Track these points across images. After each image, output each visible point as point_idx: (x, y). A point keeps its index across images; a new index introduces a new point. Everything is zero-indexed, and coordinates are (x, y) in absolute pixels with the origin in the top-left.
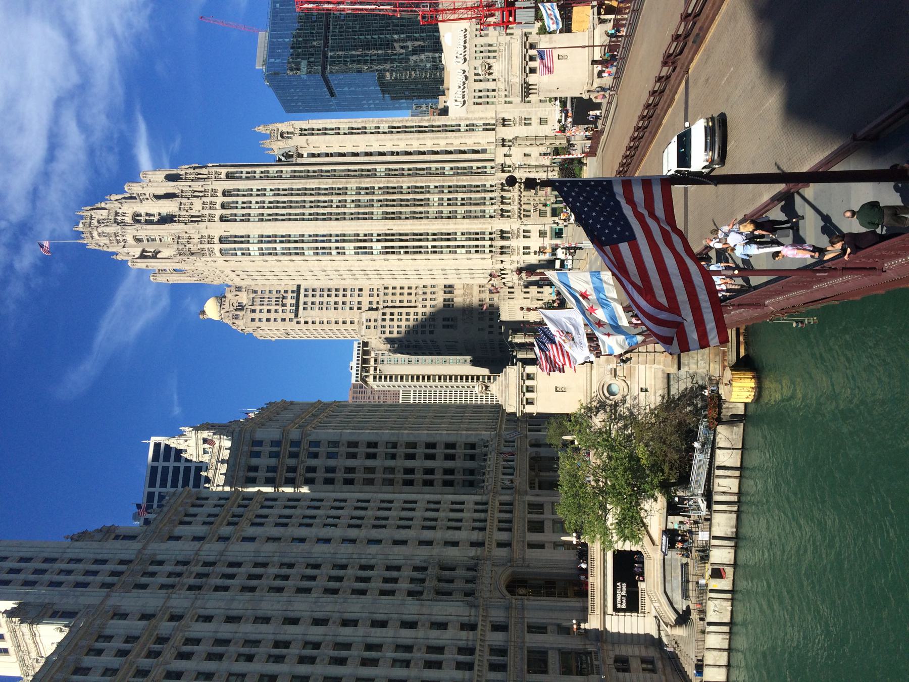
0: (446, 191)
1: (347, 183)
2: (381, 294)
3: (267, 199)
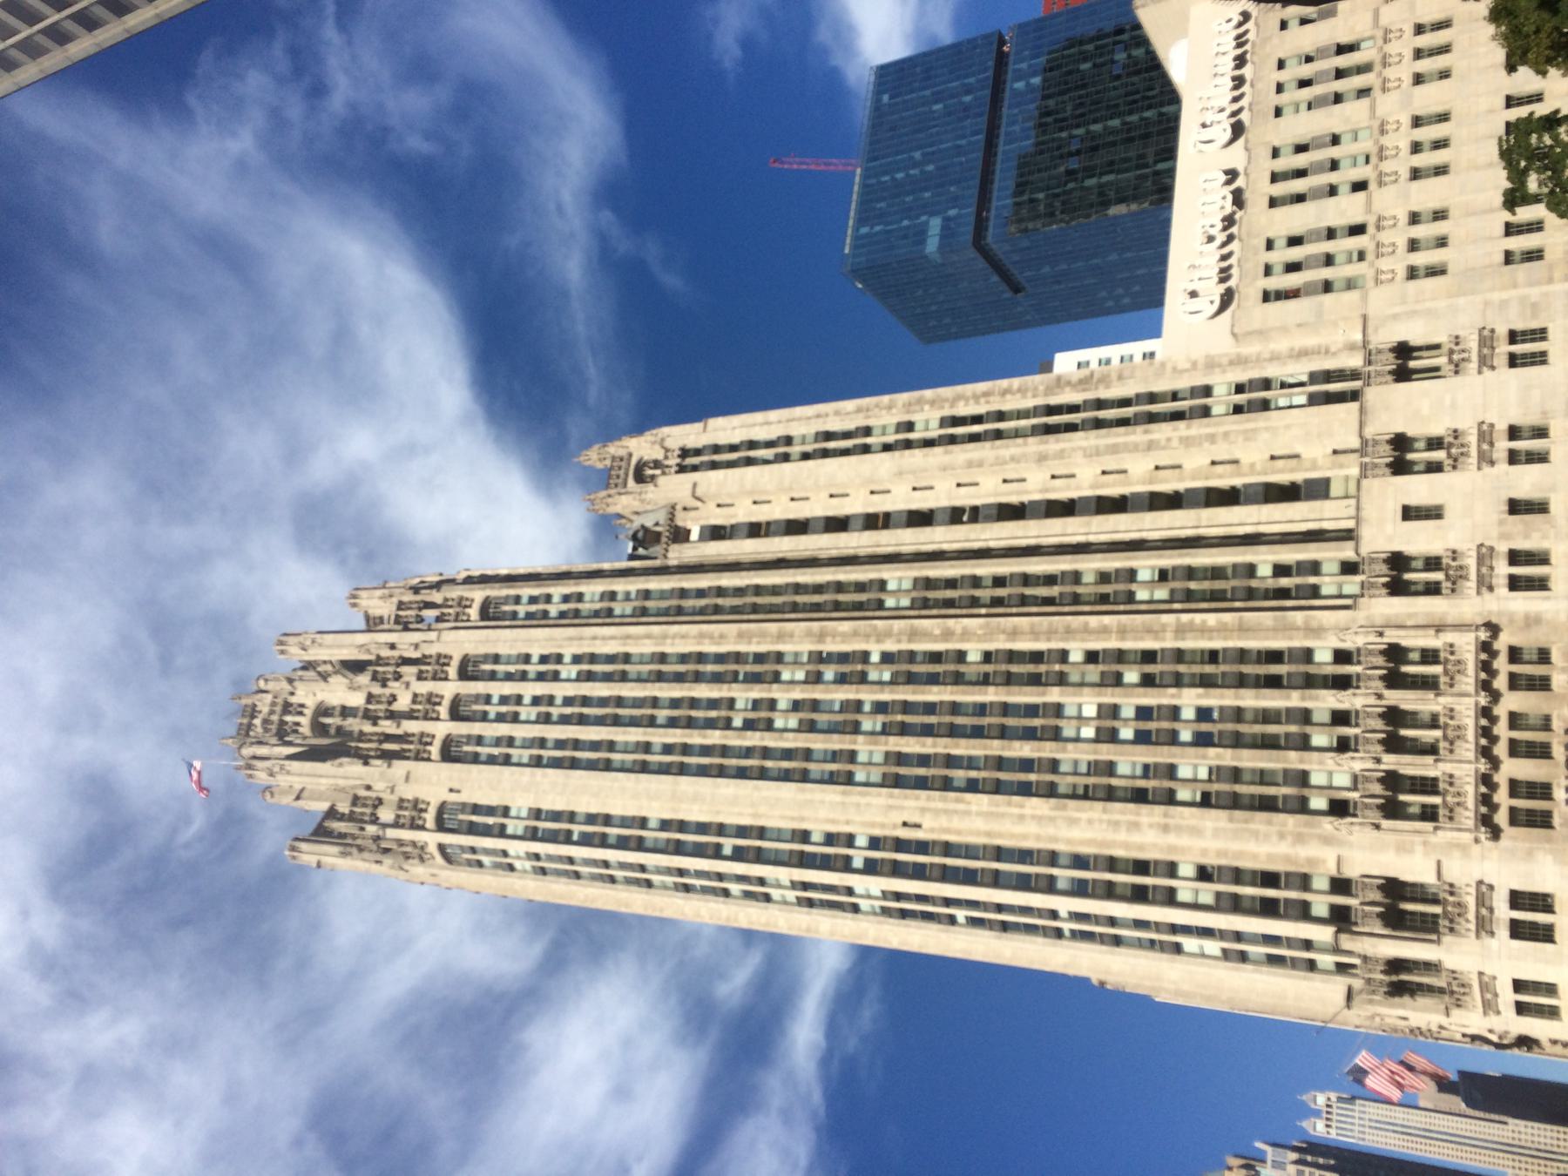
0: (1131, 676)
1: (781, 637)
3: (560, 690)
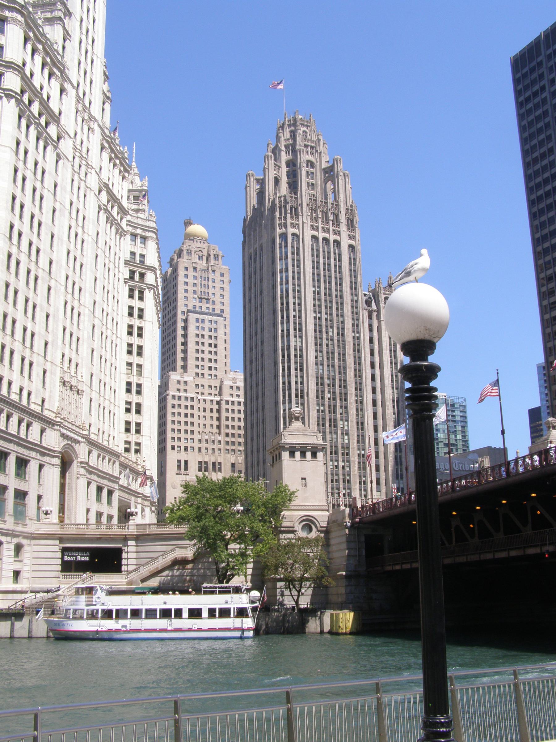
2: (212, 398)
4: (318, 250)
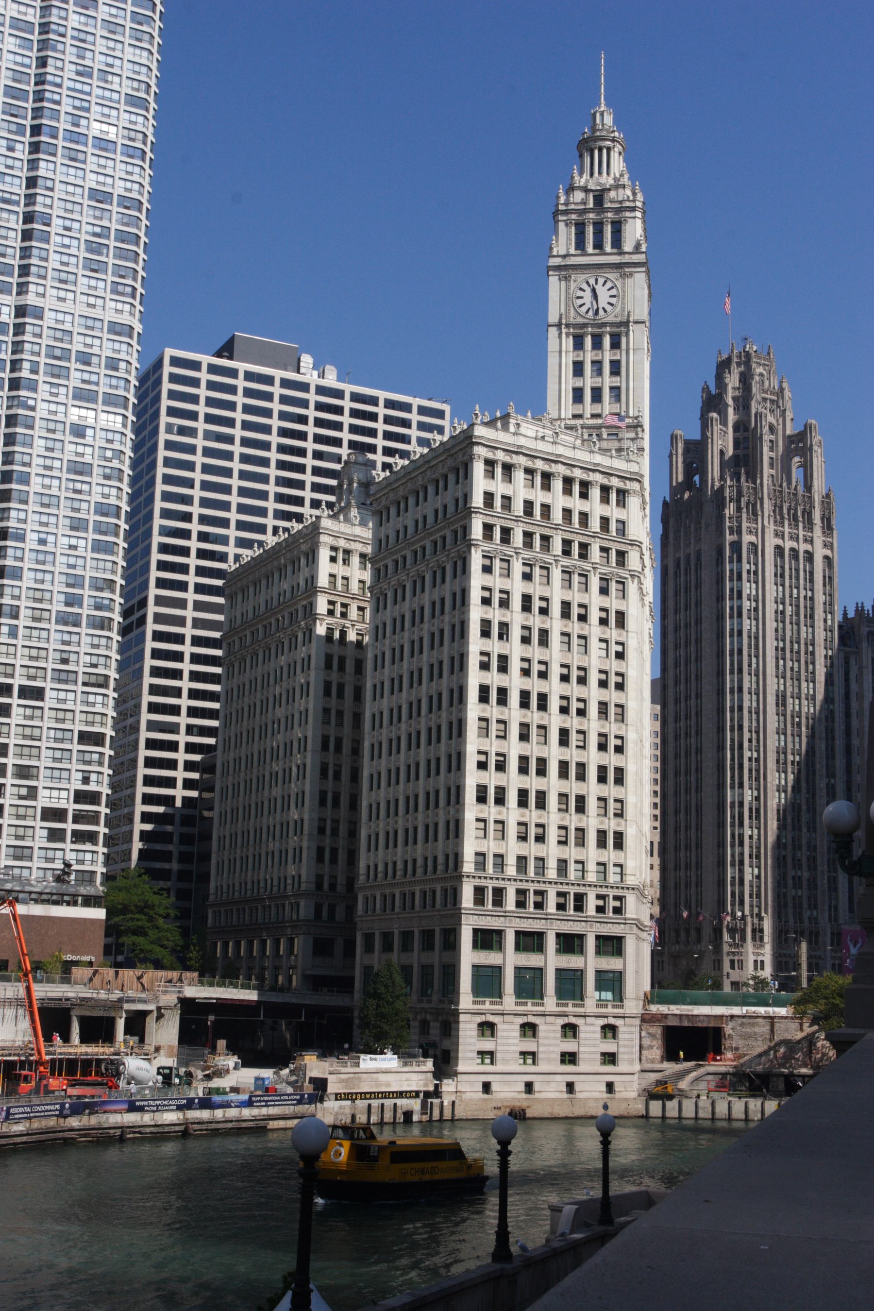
4: (783, 567)
